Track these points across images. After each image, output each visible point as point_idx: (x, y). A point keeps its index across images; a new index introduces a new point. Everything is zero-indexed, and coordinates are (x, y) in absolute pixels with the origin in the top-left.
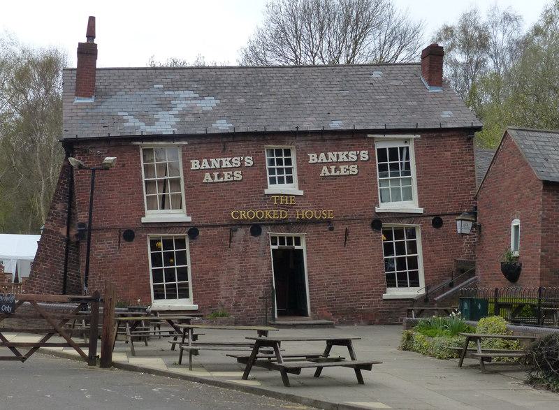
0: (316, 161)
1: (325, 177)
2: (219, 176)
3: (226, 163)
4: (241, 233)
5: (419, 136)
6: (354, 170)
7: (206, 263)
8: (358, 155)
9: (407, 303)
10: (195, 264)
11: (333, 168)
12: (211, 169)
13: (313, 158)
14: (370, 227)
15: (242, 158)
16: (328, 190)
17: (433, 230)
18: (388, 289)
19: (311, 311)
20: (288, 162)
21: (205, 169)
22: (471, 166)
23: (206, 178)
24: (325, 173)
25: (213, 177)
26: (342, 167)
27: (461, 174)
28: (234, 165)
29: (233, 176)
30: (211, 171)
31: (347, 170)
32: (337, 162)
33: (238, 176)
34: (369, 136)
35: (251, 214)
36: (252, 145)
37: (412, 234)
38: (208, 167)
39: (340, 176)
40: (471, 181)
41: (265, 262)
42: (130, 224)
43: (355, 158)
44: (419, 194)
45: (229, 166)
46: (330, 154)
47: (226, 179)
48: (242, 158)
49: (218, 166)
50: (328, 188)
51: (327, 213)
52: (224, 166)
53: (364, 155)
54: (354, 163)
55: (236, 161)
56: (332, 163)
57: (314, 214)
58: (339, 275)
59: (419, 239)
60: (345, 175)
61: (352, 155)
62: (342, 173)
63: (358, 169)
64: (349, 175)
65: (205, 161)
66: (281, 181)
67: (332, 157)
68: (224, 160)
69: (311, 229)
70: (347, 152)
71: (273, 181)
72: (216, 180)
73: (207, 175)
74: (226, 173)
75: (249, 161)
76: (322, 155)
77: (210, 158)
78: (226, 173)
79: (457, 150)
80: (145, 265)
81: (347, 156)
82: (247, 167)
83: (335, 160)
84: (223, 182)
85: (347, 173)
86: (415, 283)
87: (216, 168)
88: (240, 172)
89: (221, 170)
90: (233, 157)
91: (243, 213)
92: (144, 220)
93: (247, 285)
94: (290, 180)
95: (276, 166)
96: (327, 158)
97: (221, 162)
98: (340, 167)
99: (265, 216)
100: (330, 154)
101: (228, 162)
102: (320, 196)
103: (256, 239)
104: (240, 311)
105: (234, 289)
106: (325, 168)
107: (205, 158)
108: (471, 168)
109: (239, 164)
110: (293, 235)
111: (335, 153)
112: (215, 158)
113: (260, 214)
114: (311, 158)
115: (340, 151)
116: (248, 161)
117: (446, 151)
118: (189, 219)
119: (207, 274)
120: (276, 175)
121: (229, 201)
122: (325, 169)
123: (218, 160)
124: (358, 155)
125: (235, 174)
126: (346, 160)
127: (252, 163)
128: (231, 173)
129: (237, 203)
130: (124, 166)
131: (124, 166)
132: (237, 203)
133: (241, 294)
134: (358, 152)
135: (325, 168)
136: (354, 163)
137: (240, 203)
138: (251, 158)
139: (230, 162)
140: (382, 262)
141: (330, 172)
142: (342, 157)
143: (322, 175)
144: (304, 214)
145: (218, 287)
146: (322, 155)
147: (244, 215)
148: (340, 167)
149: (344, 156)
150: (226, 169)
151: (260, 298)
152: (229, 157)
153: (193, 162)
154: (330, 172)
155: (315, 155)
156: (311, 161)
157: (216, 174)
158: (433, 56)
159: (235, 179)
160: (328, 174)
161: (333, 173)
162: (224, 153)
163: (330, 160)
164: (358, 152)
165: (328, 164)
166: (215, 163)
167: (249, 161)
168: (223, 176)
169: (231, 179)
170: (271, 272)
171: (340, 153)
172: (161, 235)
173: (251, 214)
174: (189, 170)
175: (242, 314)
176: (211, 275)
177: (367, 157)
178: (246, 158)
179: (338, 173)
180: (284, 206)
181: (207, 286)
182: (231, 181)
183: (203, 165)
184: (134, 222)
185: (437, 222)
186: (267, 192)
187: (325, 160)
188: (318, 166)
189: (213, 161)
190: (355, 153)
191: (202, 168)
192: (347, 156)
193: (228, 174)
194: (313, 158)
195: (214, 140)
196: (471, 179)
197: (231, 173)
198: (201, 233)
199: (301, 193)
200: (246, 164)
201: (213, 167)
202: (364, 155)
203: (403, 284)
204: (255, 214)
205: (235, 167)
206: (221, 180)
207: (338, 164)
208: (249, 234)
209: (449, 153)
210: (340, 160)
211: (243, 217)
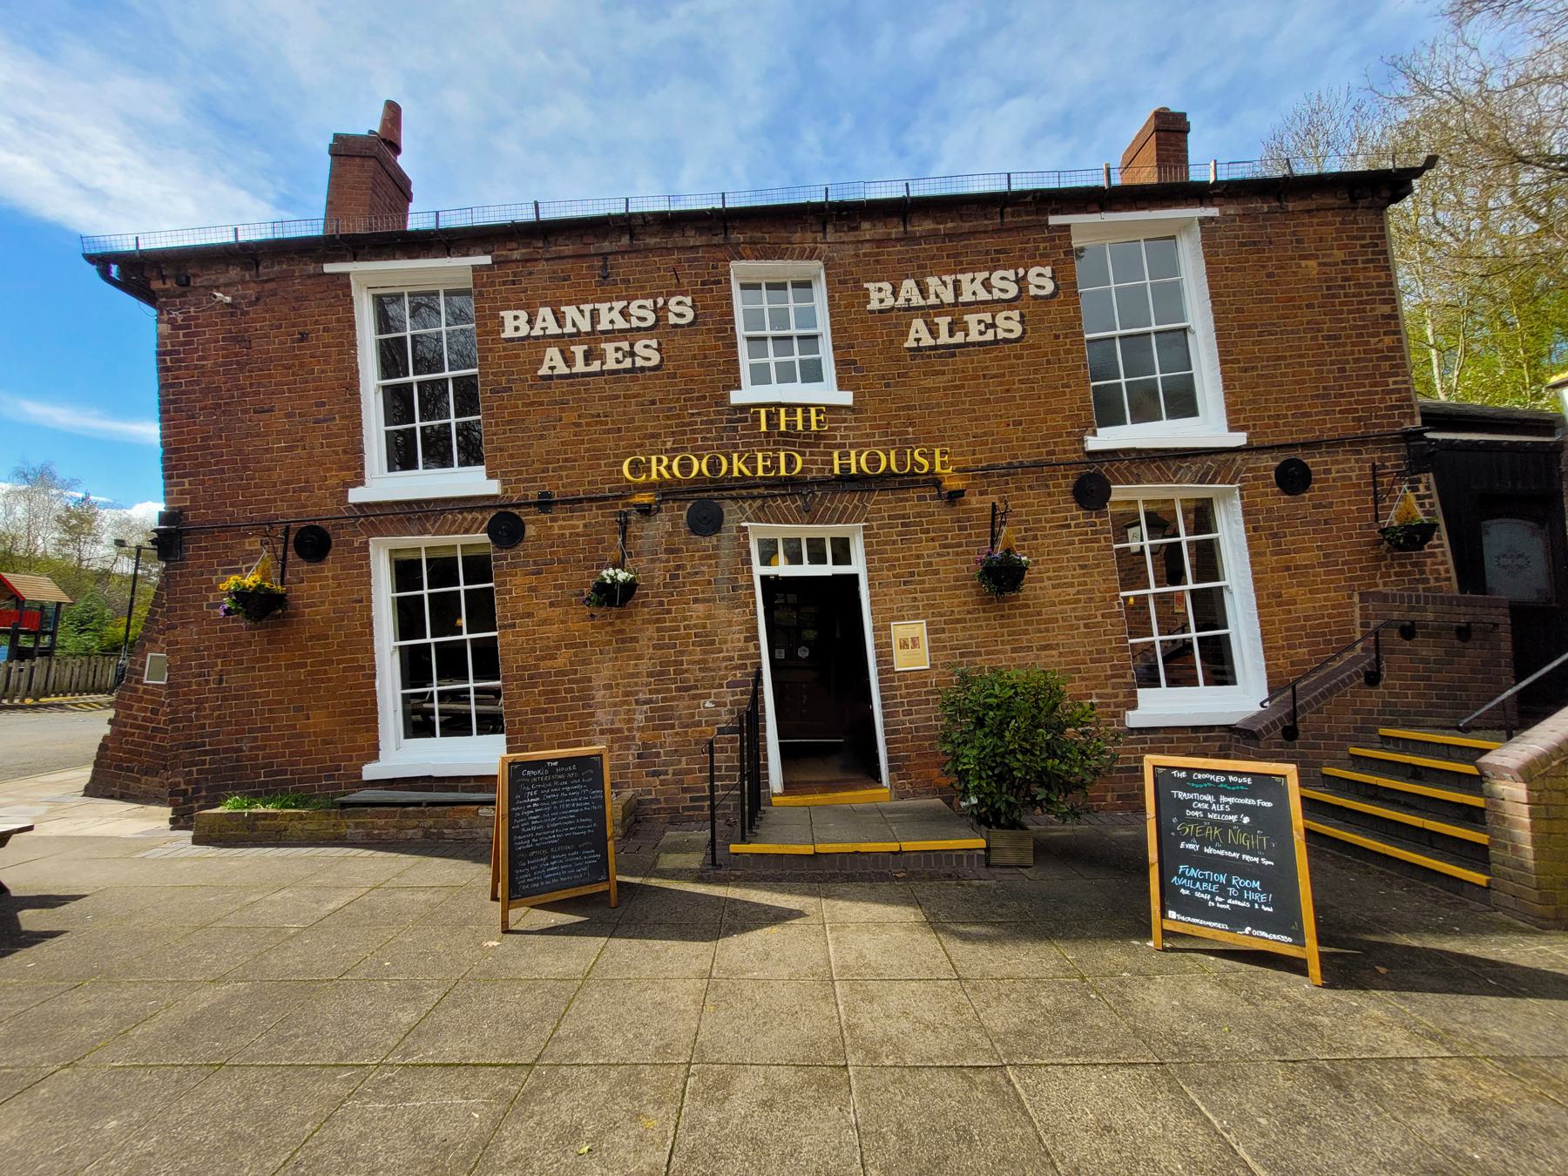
0: (889, 302)
1: (919, 349)
2: (588, 358)
3: (610, 316)
4: (661, 524)
5: (1213, 212)
6: (1009, 325)
7: (544, 622)
8: (1021, 282)
9: (1206, 739)
10: (513, 626)
11: (943, 322)
12: (563, 335)
13: (879, 295)
14: (1070, 497)
15: (660, 301)
16: (929, 390)
17: (1280, 502)
18: (1142, 693)
19: (891, 769)
20: (808, 317)
21: (544, 336)
22: (1385, 302)
23: (547, 364)
24: (918, 340)
25: (568, 360)
26: (971, 319)
27: (1355, 327)
28: (635, 323)
29: (632, 354)
30: (564, 342)
31: (988, 326)
32: (956, 304)
33: (647, 353)
34: (1054, 220)
35: (686, 466)
36: (688, 260)
37: (1202, 517)
38: (553, 329)
39: (966, 345)
40: (1390, 349)
41: (738, 615)
42: (315, 507)
43: (1013, 290)
44: (1226, 387)
45: (621, 324)
46: (932, 282)
47: (611, 365)
48: (660, 301)
49: (585, 326)
50: (929, 382)
51: (929, 456)
52: (604, 325)
53: (1040, 281)
54: (1009, 304)
55: (642, 311)
56: (940, 308)
57: (888, 461)
58: (979, 654)
59: (1230, 534)
60: (981, 344)
61: (1004, 283)
62: (974, 336)
63: (1022, 322)
64: (996, 342)
65: (545, 312)
66: (786, 375)
67: (940, 289)
68: (603, 307)
69: (882, 504)
70: (986, 274)
71: (760, 376)
72: (580, 367)
73: (553, 353)
74: (609, 348)
75: (681, 310)
76: (909, 285)
77: (561, 303)
78: (609, 348)
79: (1339, 255)
80: (362, 634)
81: (987, 285)
82: (676, 326)
83: (948, 296)
84: (602, 373)
85: (989, 336)
86: (1220, 670)
87: (579, 333)
88: (654, 343)
89: (594, 339)
90: (630, 299)
91: (660, 461)
92: (356, 496)
93: (678, 689)
94: (812, 373)
95: (768, 332)
96: (924, 292)
97: (595, 315)
98: (966, 317)
99: (730, 470)
100: (932, 282)
101: (616, 315)
102: (903, 408)
103: (706, 542)
104: (655, 774)
105: (637, 702)
106: (918, 324)
107: (544, 304)
108: (1386, 309)
109: (651, 319)
110: (827, 531)
111: (948, 279)
112: (577, 302)
113: (714, 466)
114: (874, 296)
115: (963, 271)
116: (679, 309)
117: (1305, 258)
118: (493, 487)
119: (553, 657)
120: (772, 359)
121: (619, 430)
122: (918, 333)
123: (587, 308)
124: (1021, 282)
125: (638, 347)
126: (983, 295)
127: (690, 315)
128: (625, 346)
129: (646, 436)
130: (304, 337)
131: (304, 337)
132: (646, 436)
133: (661, 718)
134: (1021, 272)
135: (918, 324)
136: (1009, 304)
137: (653, 436)
138: (688, 300)
139: (624, 313)
140: (1117, 609)
141: (934, 333)
142: (972, 288)
143: (910, 343)
144: (857, 462)
145: (586, 698)
146: (909, 285)
147: (660, 468)
148: (966, 317)
149: (977, 286)
150: (611, 335)
151: (721, 731)
152: (618, 299)
153: (507, 315)
154: (934, 333)
155: (887, 286)
156: (874, 305)
157: (579, 351)
158: (1162, 134)
159: (639, 363)
160: (927, 341)
161: (944, 338)
162: (607, 285)
163: (932, 300)
164: (1021, 272)
165: (928, 313)
166: (577, 318)
167: (681, 310)
168: (602, 357)
169: (627, 363)
170: (758, 647)
171: (965, 278)
172: (422, 543)
173: (686, 466)
174: (498, 340)
175: (663, 783)
176: (563, 659)
177: (1050, 287)
178: (673, 301)
179: (959, 338)
180: (790, 438)
181: (552, 696)
182: (626, 371)
183: (539, 324)
184: (331, 504)
185: (1293, 478)
186: (736, 398)
187: (917, 300)
188: (897, 319)
189: (570, 311)
190: (1010, 274)
191: (537, 332)
192: (987, 285)
193: (617, 349)
194: (879, 295)
195: (568, 248)
196: (1388, 340)
197: (625, 346)
198: (530, 531)
199: (846, 398)
200: (673, 320)
201: (569, 329)
202: (1040, 281)
203: (1181, 677)
204: (699, 466)
205: (638, 329)
206: (596, 366)
207: (957, 311)
208: (683, 528)
209: (1312, 263)
210: (966, 297)
211: (659, 474)
